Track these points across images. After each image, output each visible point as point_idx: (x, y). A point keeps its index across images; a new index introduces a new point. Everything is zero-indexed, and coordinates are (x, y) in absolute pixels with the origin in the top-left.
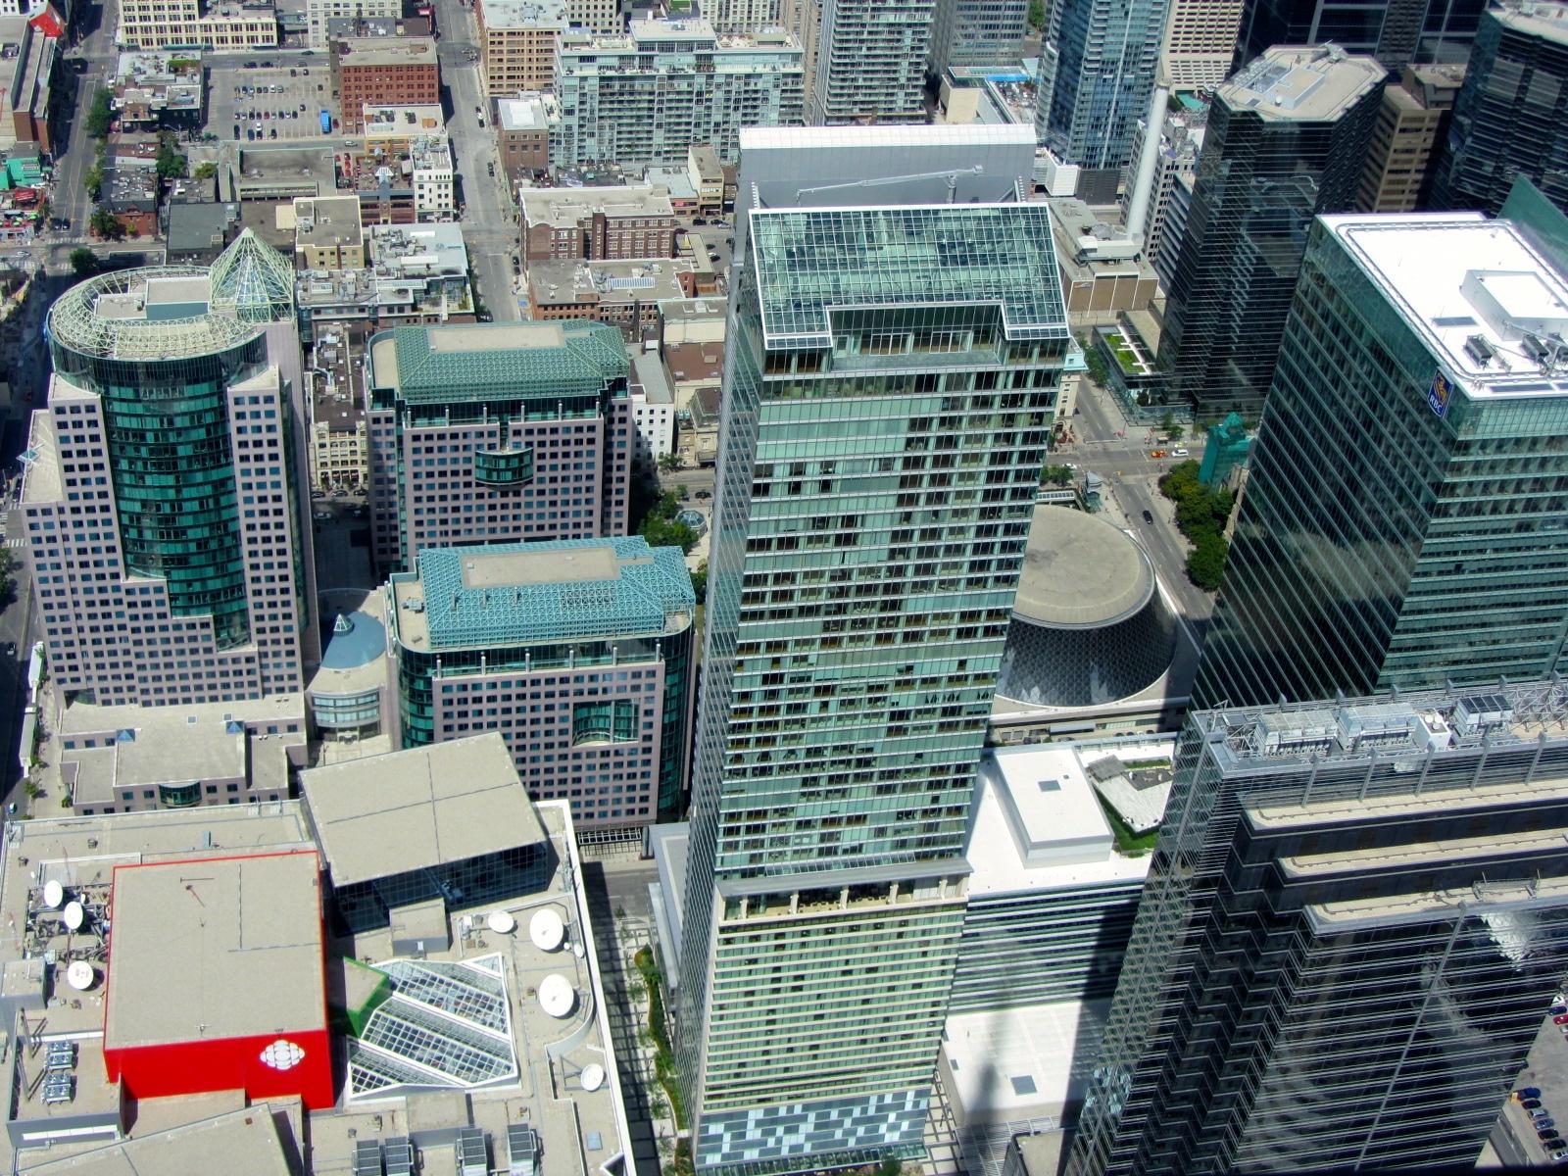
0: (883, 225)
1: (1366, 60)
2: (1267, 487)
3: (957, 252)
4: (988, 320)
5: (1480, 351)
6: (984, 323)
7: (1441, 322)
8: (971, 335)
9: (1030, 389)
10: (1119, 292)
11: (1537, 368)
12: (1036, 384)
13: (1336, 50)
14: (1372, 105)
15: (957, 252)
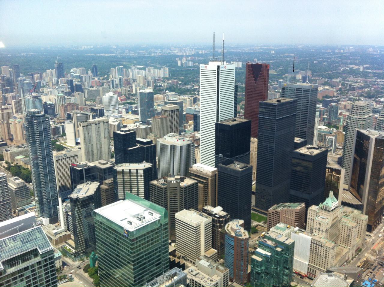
0: (8, 241)
1: (96, 182)
2: (102, 263)
3: (25, 241)
4: (36, 251)
5: (130, 223)
6: (35, 253)
7: (121, 220)
8: (33, 256)
9: (48, 262)
10: (65, 239)
11: (140, 222)
12: (49, 260)
13: (89, 182)
14: (99, 189)
15: (25, 241)
